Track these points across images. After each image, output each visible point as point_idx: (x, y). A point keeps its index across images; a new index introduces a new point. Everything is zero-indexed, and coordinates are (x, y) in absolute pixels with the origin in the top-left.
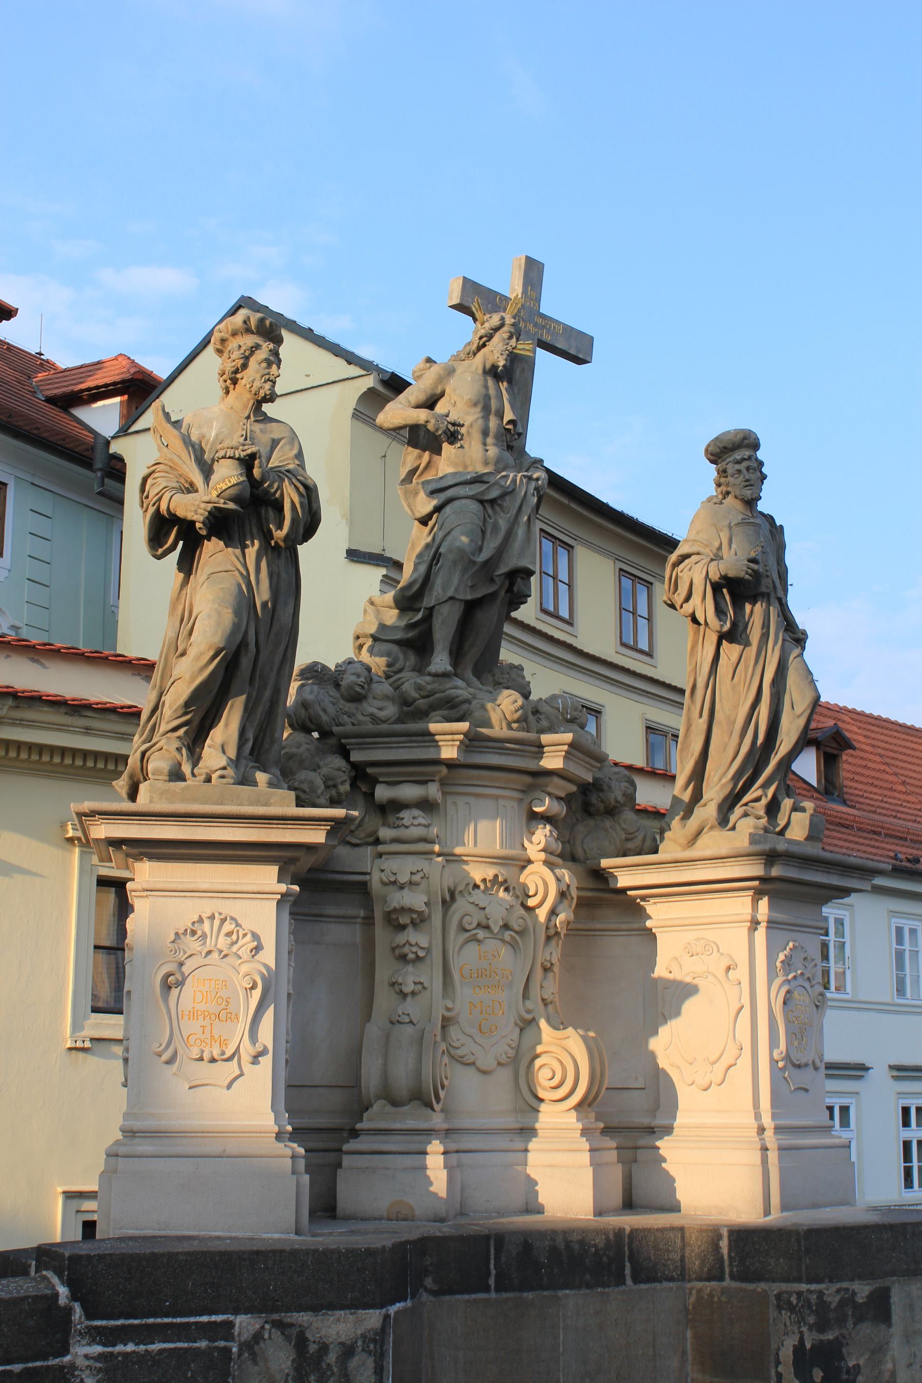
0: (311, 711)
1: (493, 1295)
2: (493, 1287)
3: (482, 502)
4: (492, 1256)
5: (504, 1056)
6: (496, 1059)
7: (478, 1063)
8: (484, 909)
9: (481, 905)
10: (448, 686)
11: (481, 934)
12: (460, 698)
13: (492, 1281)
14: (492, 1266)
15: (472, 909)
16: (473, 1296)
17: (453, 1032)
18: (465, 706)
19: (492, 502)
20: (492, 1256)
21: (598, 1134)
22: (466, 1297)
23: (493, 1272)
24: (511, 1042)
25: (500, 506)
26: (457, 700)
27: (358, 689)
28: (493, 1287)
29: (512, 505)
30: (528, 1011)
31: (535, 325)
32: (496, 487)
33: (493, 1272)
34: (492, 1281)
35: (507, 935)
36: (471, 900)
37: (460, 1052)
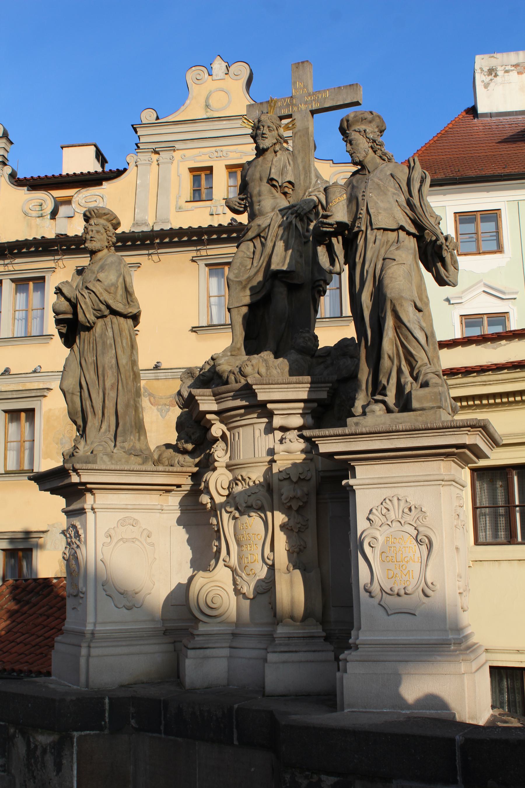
1: (163, 736)
2: (163, 732)
4: (163, 713)
13: (162, 728)
14: (162, 719)
16: (154, 735)
20: (163, 713)
21: (323, 640)
22: (150, 734)
23: (163, 722)
28: (163, 732)
33: (163, 722)
34: (162, 728)
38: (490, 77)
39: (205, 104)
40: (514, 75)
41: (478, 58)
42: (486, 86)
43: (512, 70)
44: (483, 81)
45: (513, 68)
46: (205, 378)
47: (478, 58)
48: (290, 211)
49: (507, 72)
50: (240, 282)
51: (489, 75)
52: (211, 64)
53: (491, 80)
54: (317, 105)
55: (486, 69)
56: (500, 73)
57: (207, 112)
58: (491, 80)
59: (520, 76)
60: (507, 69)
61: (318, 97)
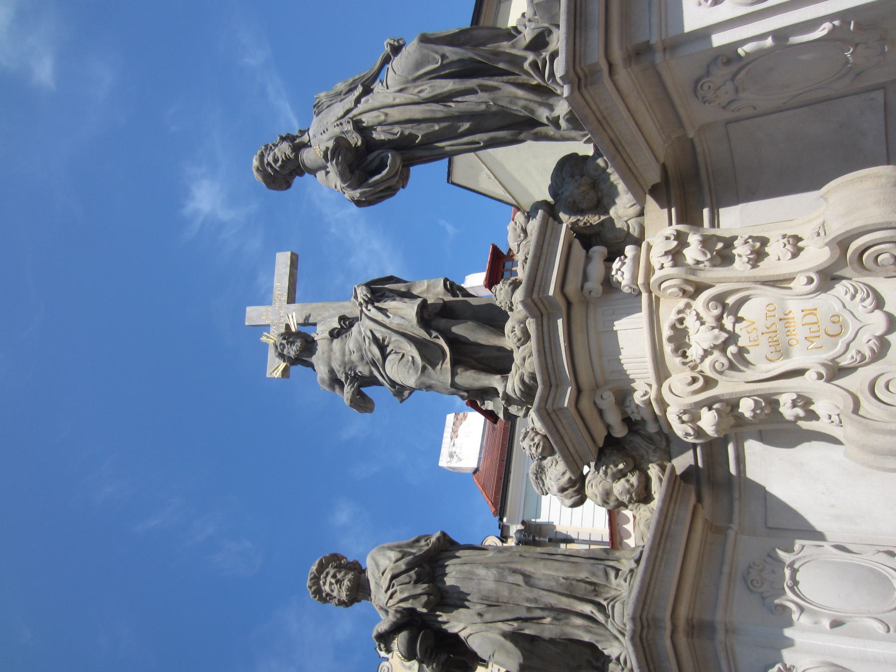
0: (566, 486)
3: (384, 357)
5: (869, 300)
6: (872, 311)
7: (879, 333)
8: (705, 351)
9: (701, 353)
10: (514, 396)
11: (732, 349)
12: (521, 387)
15: (708, 360)
17: (845, 362)
18: (527, 380)
19: (382, 347)
24: (849, 296)
25: (384, 340)
26: (523, 389)
27: (540, 450)
29: (380, 333)
30: (810, 281)
31: (280, 308)
32: (371, 349)
35: (728, 322)
36: (698, 361)
37: (868, 354)
38: (455, 457)
39: (407, 670)
40: (456, 440)
41: (441, 464)
42: (460, 460)
43: (454, 441)
44: (456, 462)
45: (453, 441)
46: (541, 444)
47: (441, 464)
48: (364, 309)
49: (454, 445)
50: (424, 369)
51: (453, 457)
52: (380, 657)
53: (457, 456)
54: (285, 295)
55: (449, 459)
56: (454, 449)
57: (414, 669)
58: (457, 456)
59: (459, 437)
60: (452, 445)
61: (279, 294)
